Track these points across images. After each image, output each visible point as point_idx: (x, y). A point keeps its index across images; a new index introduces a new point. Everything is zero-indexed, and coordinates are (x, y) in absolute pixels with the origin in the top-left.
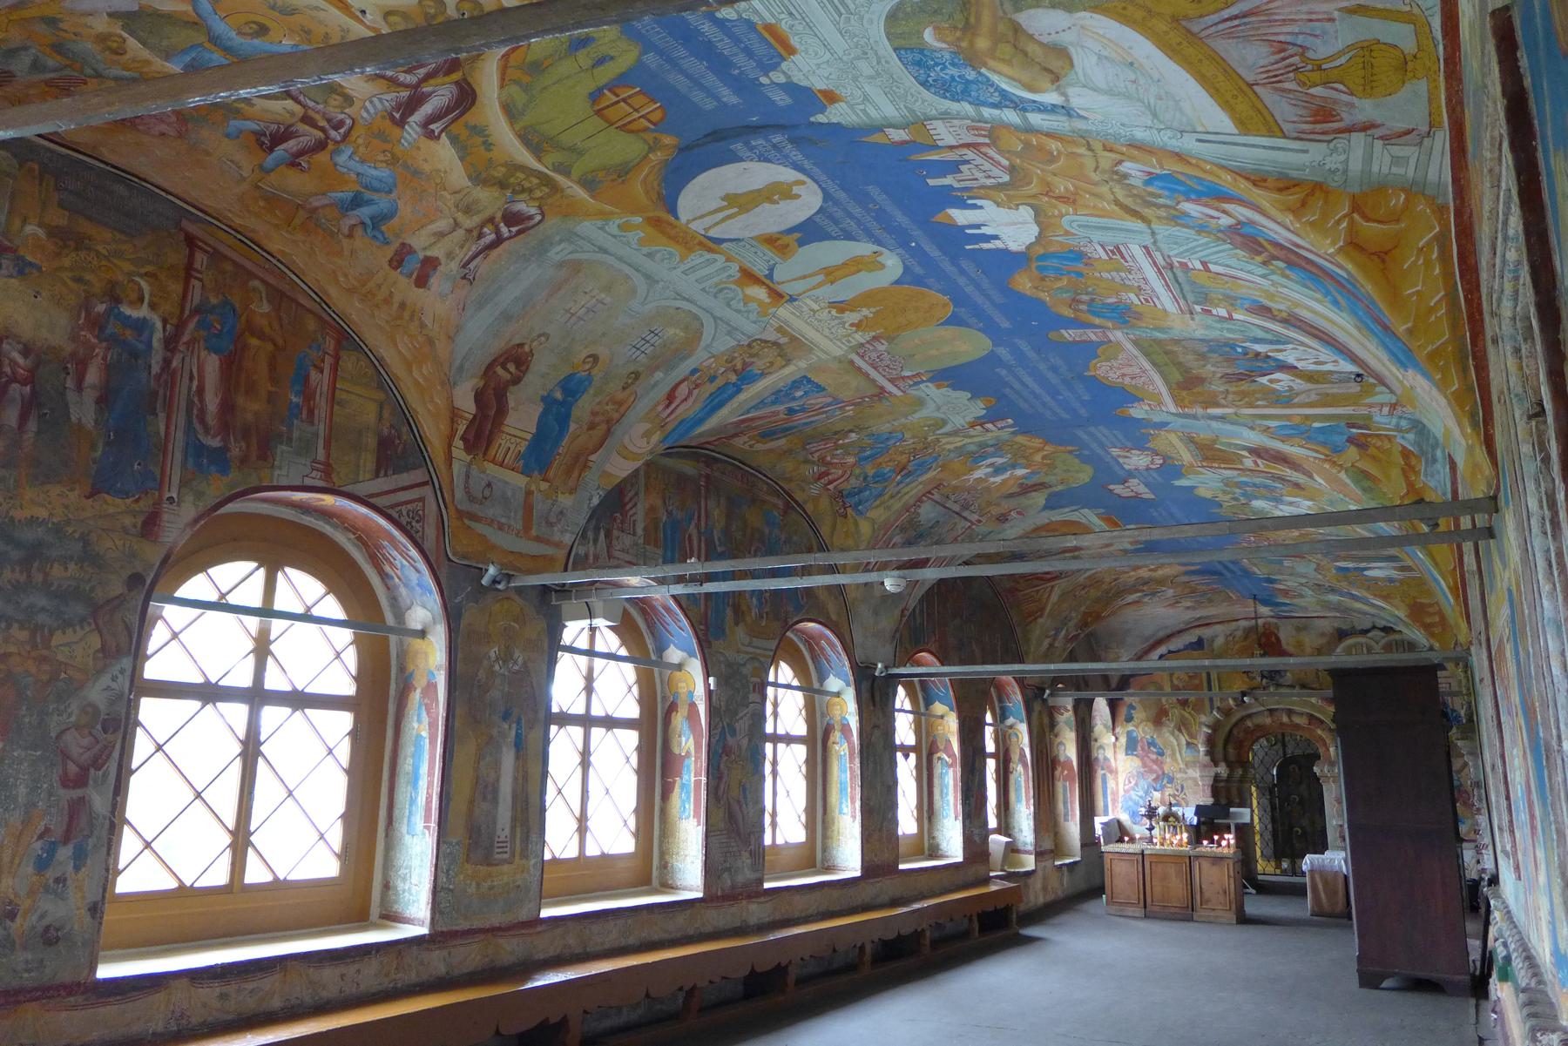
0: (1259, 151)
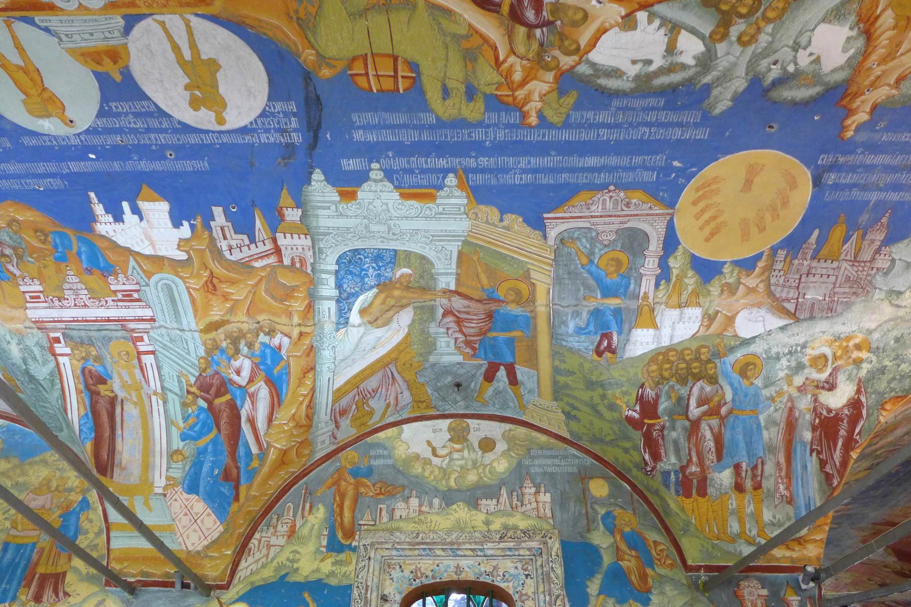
0: (324, 400)
